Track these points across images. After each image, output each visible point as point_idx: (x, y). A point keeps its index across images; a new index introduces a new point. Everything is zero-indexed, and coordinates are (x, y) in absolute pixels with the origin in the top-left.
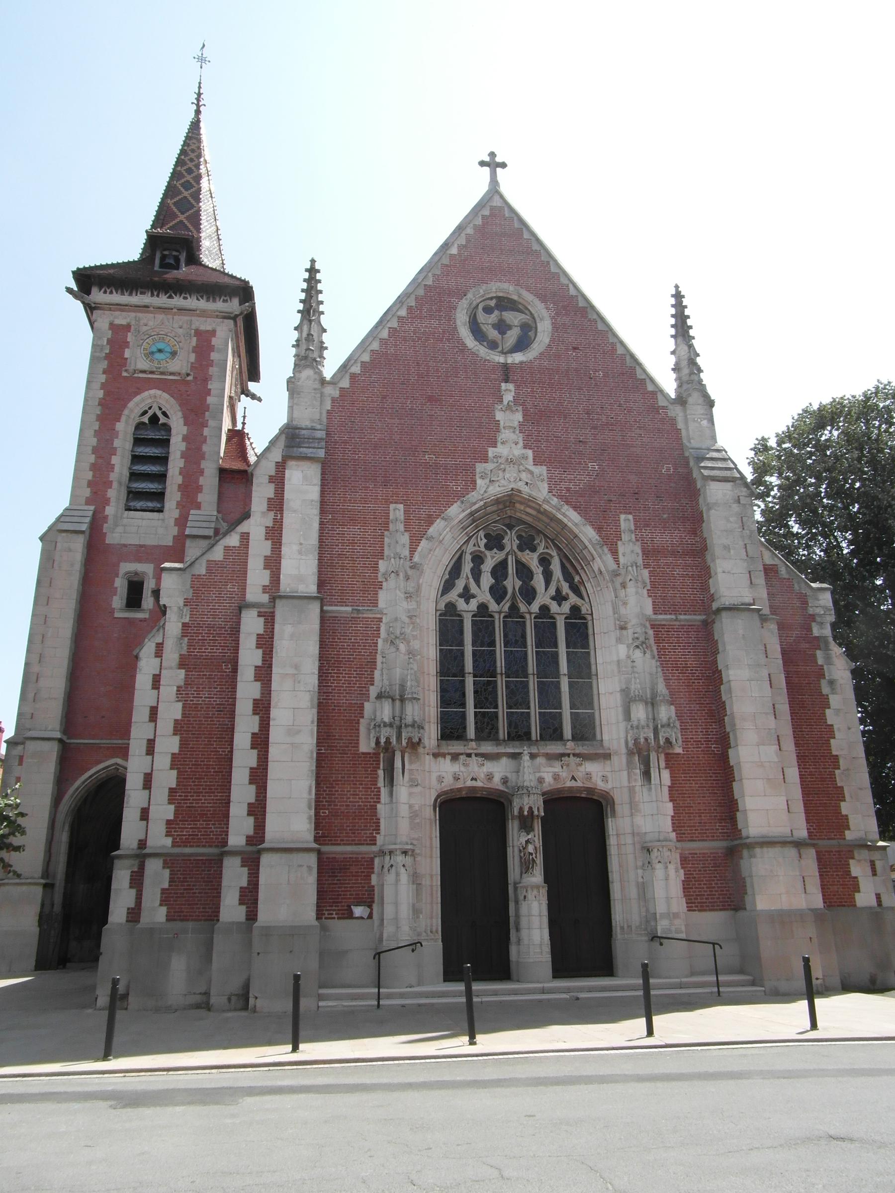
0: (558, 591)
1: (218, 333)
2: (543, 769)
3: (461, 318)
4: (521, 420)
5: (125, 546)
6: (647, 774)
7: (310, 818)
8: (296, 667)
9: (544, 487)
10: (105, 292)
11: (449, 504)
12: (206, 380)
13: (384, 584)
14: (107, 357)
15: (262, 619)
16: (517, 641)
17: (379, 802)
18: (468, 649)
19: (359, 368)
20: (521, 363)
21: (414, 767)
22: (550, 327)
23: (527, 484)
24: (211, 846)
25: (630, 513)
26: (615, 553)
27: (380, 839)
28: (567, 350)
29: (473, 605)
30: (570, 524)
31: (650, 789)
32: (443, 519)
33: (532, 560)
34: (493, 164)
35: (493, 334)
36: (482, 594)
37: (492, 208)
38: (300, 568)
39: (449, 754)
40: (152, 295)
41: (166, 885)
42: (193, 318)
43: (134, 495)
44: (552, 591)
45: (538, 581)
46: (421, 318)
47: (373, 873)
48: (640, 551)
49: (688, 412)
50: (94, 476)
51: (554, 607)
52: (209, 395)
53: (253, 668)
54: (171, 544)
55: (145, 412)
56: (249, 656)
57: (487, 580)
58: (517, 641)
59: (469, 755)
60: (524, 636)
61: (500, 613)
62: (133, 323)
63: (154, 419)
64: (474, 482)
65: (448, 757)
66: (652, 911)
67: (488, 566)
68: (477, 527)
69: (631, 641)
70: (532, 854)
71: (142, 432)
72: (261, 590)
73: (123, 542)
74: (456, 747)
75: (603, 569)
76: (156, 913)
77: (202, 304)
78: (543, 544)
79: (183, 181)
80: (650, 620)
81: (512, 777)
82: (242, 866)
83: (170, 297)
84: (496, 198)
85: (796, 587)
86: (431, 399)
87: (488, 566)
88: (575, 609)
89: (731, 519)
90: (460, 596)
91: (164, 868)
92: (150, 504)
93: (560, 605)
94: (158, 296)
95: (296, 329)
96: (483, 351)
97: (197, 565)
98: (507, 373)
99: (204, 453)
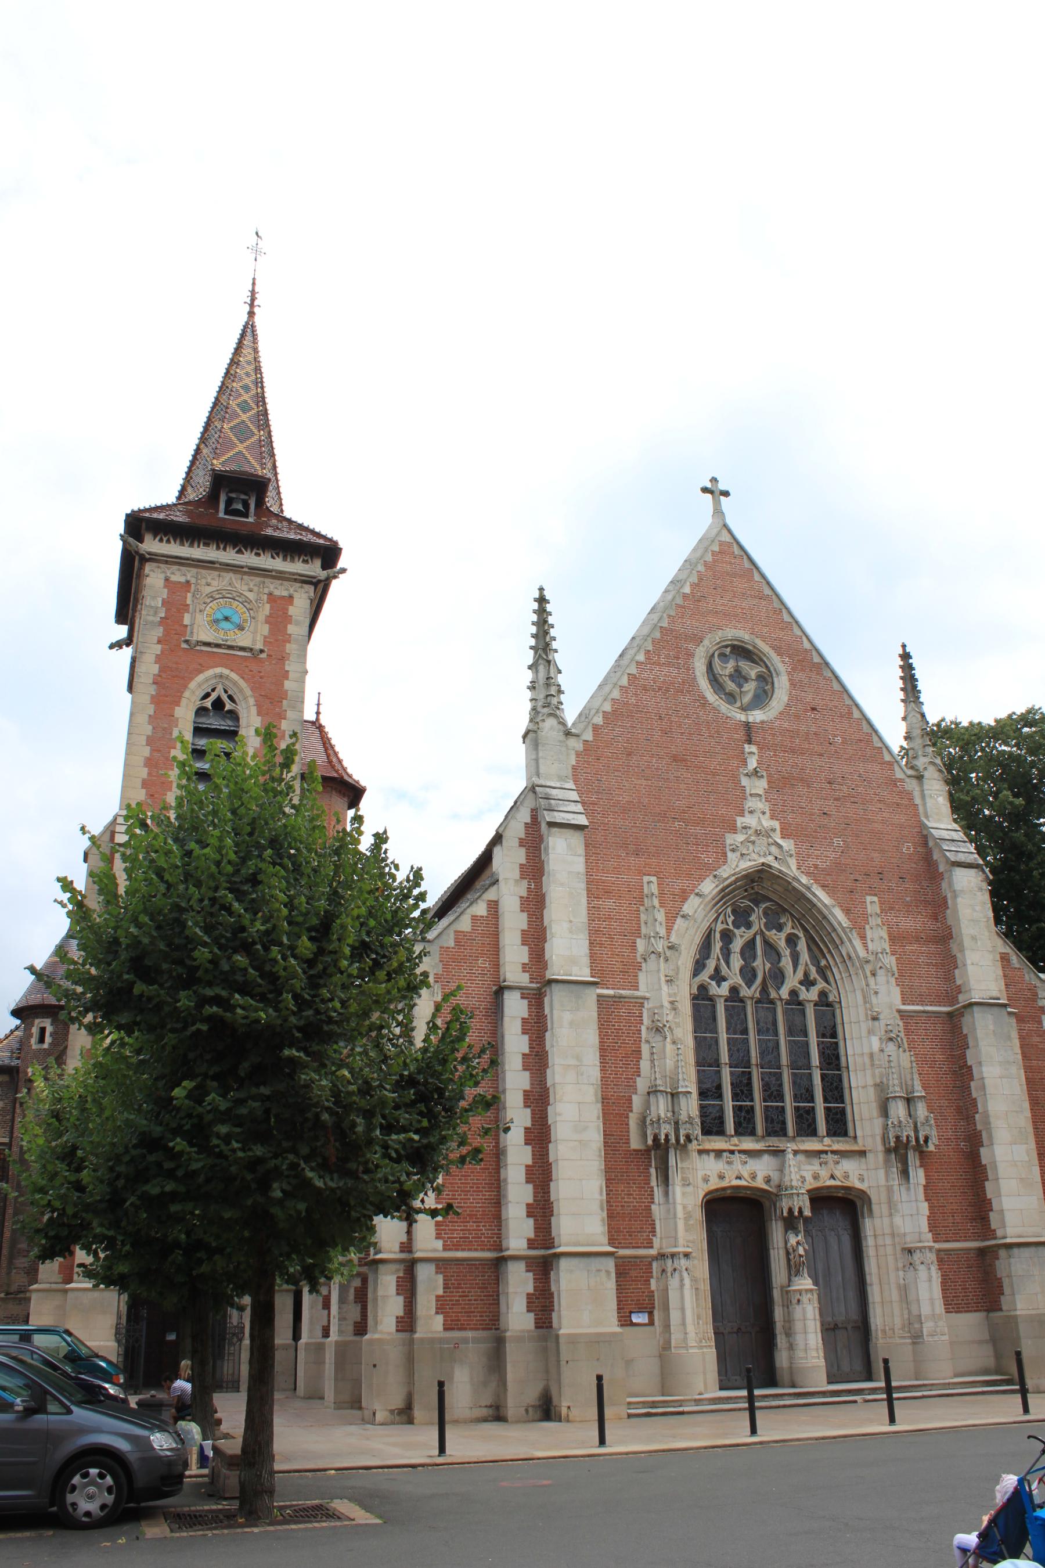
0: (806, 974)
1: (295, 601)
2: (803, 1167)
3: (700, 667)
4: (766, 787)
6: (905, 1173)
7: (603, 1220)
8: (578, 1058)
9: (793, 863)
10: (161, 540)
11: (702, 879)
12: (282, 659)
13: (644, 965)
14: (163, 621)
15: (526, 1002)
16: (768, 1030)
17: (653, 1203)
18: (723, 1037)
19: (601, 719)
20: (762, 722)
21: (685, 1165)
22: (788, 684)
23: (776, 858)
24: (482, 1250)
25: (875, 895)
26: (863, 937)
27: (656, 1242)
28: (806, 711)
29: (724, 990)
30: (819, 905)
31: (908, 1189)
32: (697, 894)
33: (780, 939)
34: (714, 491)
35: (731, 686)
36: (735, 978)
37: (721, 544)
38: (568, 950)
39: (713, 1151)
40: (218, 548)
41: (441, 1292)
42: (267, 580)
44: (800, 974)
45: (786, 963)
46: (659, 664)
47: (652, 1277)
48: (886, 936)
49: (925, 787)
50: (149, 774)
51: (804, 994)
52: (287, 679)
53: (521, 1056)
55: (207, 696)
56: (515, 1044)
57: (737, 962)
58: (768, 1030)
59: (732, 1152)
60: (775, 1023)
61: (752, 998)
62: (193, 581)
63: (218, 704)
64: (725, 855)
65: (712, 1155)
66: (915, 1312)
67: (737, 945)
68: (725, 903)
69: (883, 1033)
70: (801, 1256)
72: (521, 970)
74: (717, 1143)
75: (853, 955)
76: (431, 1323)
77: (278, 564)
78: (790, 924)
79: (239, 400)
80: (899, 1011)
81: (775, 1176)
82: (528, 1271)
83: (239, 552)
84: (725, 532)
85: (1027, 977)
86: (675, 759)
87: (737, 945)
88: (823, 994)
89: (978, 908)
90: (711, 978)
91: (437, 1273)
93: (808, 990)
94: (225, 549)
95: (530, 667)
96: (724, 707)
97: (444, 937)
98: (749, 731)
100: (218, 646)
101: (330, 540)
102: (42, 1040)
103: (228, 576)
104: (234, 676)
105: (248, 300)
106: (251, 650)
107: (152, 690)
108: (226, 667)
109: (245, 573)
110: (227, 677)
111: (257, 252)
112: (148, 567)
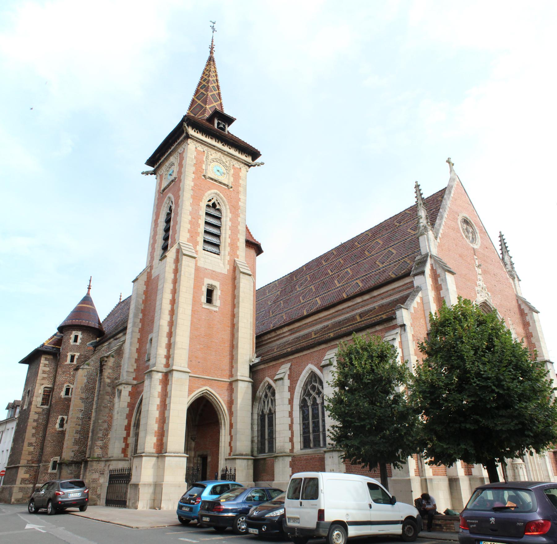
5: (206, 269)
12: (238, 193)
14: (195, 164)
50: (191, 227)
54: (226, 273)
55: (210, 201)
62: (206, 152)
63: (214, 205)
71: (208, 210)
73: (205, 267)
77: (236, 154)
83: (223, 145)
86: (460, 256)
99: (239, 230)
100: (216, 181)
102: (76, 340)
104: (221, 195)
106: (228, 186)
107: (191, 193)
109: (225, 154)
111: (214, 30)
112: (189, 141)
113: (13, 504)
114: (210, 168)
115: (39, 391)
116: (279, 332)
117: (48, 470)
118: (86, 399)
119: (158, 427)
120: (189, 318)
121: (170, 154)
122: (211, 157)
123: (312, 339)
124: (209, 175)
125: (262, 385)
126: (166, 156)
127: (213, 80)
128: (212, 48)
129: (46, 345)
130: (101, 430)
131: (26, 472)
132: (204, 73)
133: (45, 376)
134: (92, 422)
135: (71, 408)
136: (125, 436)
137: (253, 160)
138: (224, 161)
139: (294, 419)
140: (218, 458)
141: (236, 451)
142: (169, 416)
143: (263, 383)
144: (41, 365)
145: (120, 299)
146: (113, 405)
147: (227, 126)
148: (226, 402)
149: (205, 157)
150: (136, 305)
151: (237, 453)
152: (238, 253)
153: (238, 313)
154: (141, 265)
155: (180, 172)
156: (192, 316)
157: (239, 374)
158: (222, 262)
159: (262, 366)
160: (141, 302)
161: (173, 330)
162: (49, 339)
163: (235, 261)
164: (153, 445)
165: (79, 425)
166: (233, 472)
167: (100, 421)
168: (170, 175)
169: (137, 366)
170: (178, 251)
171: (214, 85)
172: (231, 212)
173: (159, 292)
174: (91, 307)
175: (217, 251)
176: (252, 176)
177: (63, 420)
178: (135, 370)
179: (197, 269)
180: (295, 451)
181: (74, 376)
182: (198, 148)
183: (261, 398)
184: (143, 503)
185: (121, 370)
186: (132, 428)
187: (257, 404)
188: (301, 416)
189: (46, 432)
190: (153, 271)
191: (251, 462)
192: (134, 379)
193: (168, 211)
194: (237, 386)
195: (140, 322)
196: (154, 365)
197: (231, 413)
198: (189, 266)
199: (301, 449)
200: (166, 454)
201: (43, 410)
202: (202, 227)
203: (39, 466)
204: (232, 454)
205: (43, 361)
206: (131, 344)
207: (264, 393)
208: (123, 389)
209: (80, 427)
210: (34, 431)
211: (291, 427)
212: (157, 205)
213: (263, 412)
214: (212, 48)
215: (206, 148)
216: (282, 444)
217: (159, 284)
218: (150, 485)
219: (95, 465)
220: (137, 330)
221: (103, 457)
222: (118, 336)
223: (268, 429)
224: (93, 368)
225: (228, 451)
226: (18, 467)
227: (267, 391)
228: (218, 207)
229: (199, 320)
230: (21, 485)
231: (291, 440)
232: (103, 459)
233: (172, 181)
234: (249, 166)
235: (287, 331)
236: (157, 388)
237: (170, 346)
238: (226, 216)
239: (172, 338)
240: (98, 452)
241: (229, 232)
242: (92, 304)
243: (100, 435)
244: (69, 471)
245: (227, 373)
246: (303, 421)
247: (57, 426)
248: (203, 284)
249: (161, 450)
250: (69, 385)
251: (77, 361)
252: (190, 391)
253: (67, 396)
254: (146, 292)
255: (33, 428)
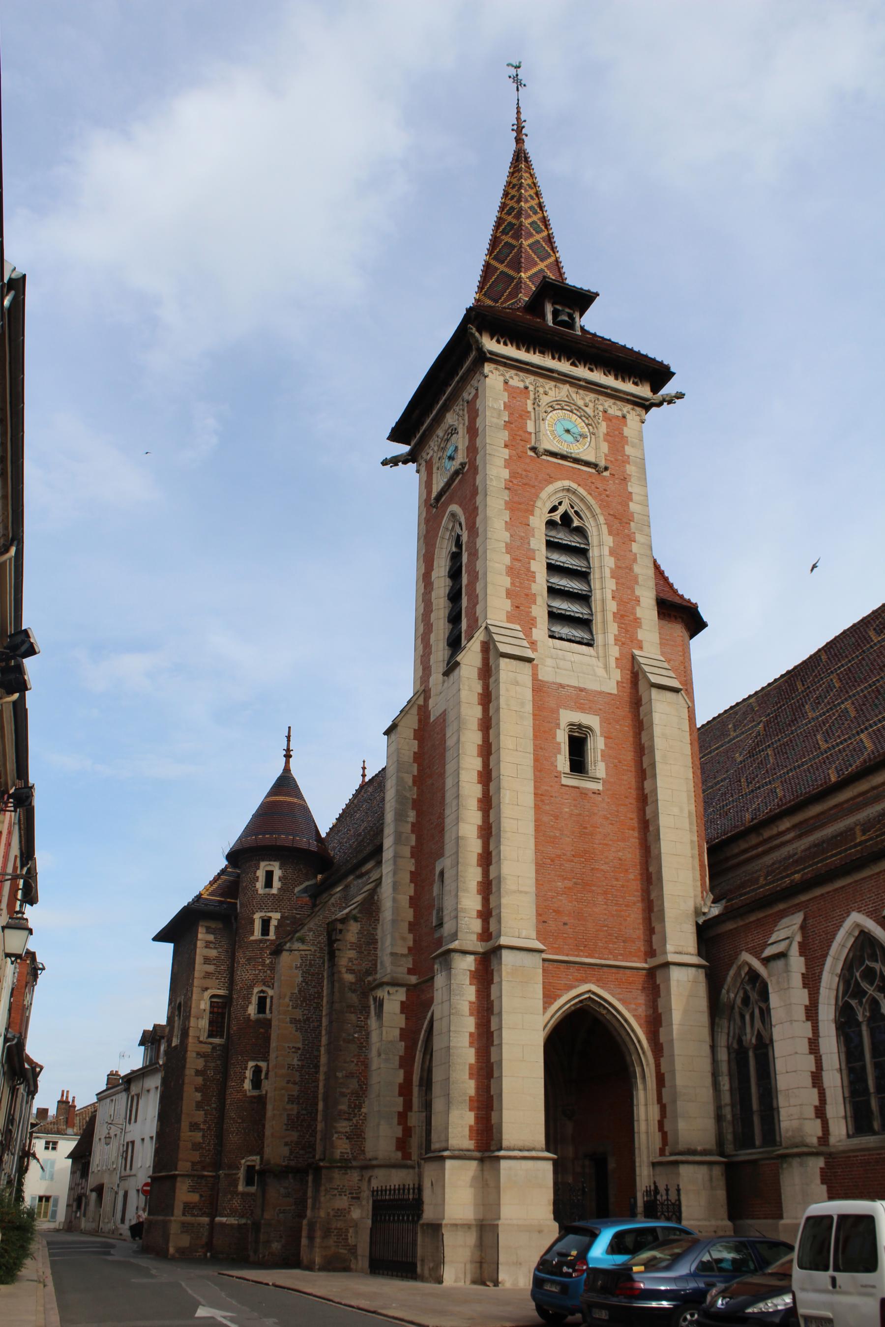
1: (629, 422)
5: (561, 686)
12: (625, 480)
42: (600, 397)
43: (554, 616)
50: (512, 584)
54: (615, 692)
55: (554, 509)
62: (531, 388)
71: (553, 533)
77: (610, 381)
92: (578, 633)
100: (564, 457)
101: (661, 363)
102: (269, 884)
103: (565, 390)
104: (581, 490)
105: (515, 127)
106: (595, 466)
107: (506, 495)
108: (574, 481)
110: (574, 492)
112: (488, 368)
113: (173, 1259)
114: (546, 427)
115: (202, 1003)
116: (767, 834)
117: (236, 1186)
118: (305, 1021)
119: (478, 1088)
120: (530, 815)
121: (445, 408)
122: (545, 400)
123: (855, 846)
124: (547, 444)
125: (732, 973)
126: (434, 412)
127: (531, 208)
128: (519, 129)
129: (204, 896)
130: (343, 1095)
131: (193, 1190)
132: (506, 194)
133: (210, 968)
134: (322, 1077)
135: (273, 1044)
136: (401, 1109)
137: (655, 390)
138: (580, 403)
139: (824, 1058)
140: (634, 1162)
141: (677, 1143)
142: (501, 1061)
143: (735, 967)
144: (199, 944)
145: (364, 776)
146: (368, 1035)
147: (577, 315)
148: (642, 1022)
149: (530, 403)
150: (397, 791)
151: (681, 1147)
152: (639, 638)
153: (655, 790)
154: (401, 689)
155: (473, 449)
156: (537, 808)
157: (669, 948)
158: (601, 664)
159: (730, 926)
160: (410, 782)
161: (491, 848)
162: (211, 883)
163: (633, 657)
164: (467, 1129)
165: (295, 1083)
166: (673, 1197)
167: (339, 1075)
168: (451, 458)
169: (415, 941)
170: (488, 647)
171: (535, 218)
172: (610, 533)
173: (449, 755)
174: (295, 800)
175: (587, 636)
176: (657, 433)
177: (257, 1071)
178: (410, 949)
179: (539, 688)
180: (832, 1140)
181: (272, 968)
182: (511, 382)
183: (733, 1008)
184: (456, 1271)
185: (379, 953)
186: (415, 1090)
187: (725, 1023)
188: (843, 1049)
189: (225, 1099)
190: (431, 702)
191: (717, 1171)
192: (410, 972)
193: (454, 549)
194: (668, 980)
195: (413, 832)
196: (454, 936)
197: (658, 1049)
198: (517, 683)
199: (849, 1136)
200: (502, 1153)
201: (214, 1048)
202: (541, 580)
203: (217, 1177)
204: (667, 1150)
205: (203, 935)
206: (396, 886)
207: (741, 994)
208: (386, 996)
209: (297, 1087)
210: (198, 1096)
211: (817, 1078)
212: (426, 537)
213: (740, 1041)
214: (519, 129)
215: (530, 379)
216: (795, 1124)
217: (449, 733)
218: (468, 1226)
219: (338, 1178)
220: (407, 851)
221: (355, 1158)
222: (364, 869)
223: (759, 1086)
224: (313, 948)
225: (658, 1144)
226: (174, 1177)
227: (748, 988)
228: (576, 523)
229: (556, 817)
230: (183, 1218)
231: (820, 1112)
232: (354, 1163)
233: (457, 473)
234: (647, 408)
235: (788, 830)
236: (468, 993)
237: (488, 888)
238: (600, 545)
239: (492, 868)
240: (342, 1147)
241: (611, 585)
242: (298, 793)
243: (343, 1107)
244: (282, 1190)
245: (640, 945)
246: (848, 1061)
247: (247, 1085)
248: (558, 726)
249: (488, 1144)
250: (264, 988)
251: (276, 933)
252: (549, 997)
253: (261, 1016)
254: (418, 757)
255: (197, 1090)
